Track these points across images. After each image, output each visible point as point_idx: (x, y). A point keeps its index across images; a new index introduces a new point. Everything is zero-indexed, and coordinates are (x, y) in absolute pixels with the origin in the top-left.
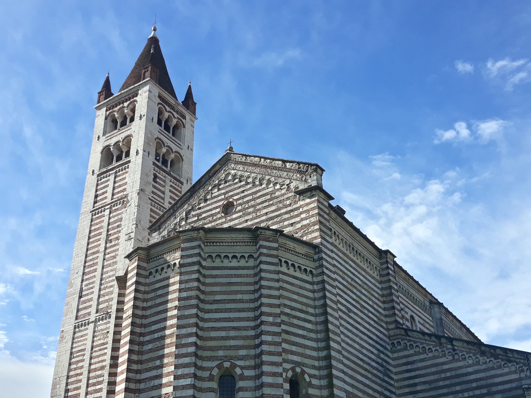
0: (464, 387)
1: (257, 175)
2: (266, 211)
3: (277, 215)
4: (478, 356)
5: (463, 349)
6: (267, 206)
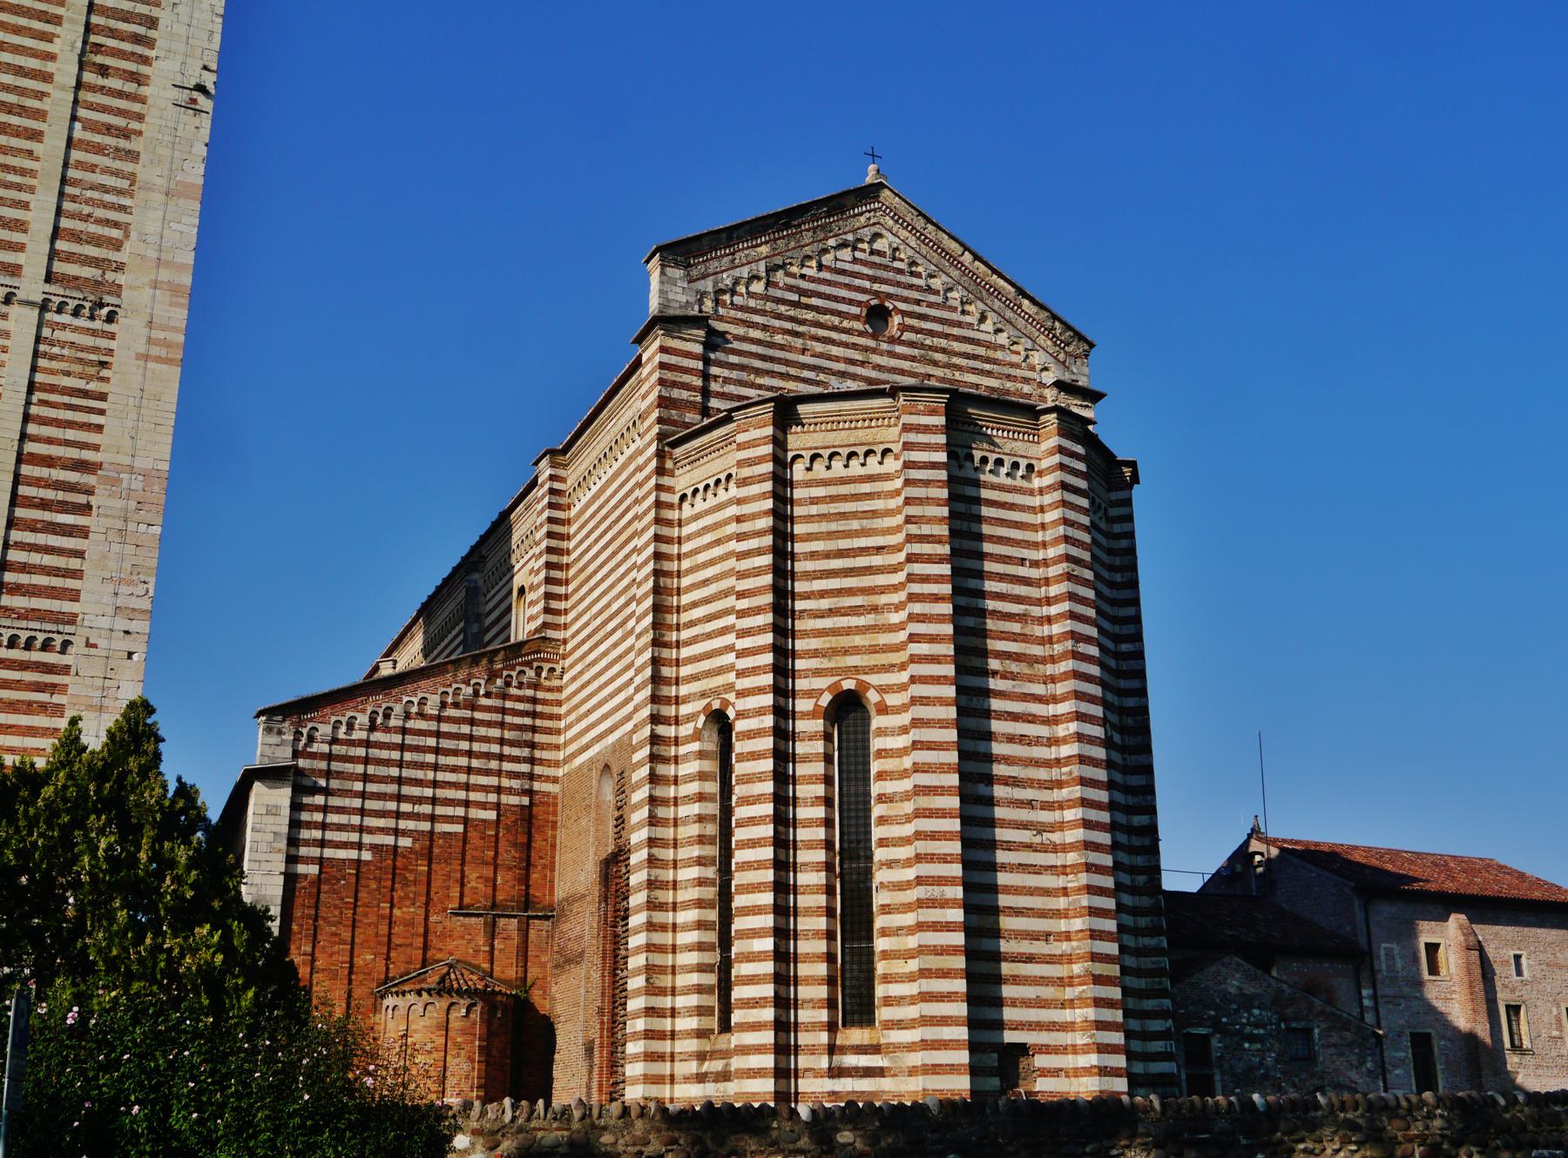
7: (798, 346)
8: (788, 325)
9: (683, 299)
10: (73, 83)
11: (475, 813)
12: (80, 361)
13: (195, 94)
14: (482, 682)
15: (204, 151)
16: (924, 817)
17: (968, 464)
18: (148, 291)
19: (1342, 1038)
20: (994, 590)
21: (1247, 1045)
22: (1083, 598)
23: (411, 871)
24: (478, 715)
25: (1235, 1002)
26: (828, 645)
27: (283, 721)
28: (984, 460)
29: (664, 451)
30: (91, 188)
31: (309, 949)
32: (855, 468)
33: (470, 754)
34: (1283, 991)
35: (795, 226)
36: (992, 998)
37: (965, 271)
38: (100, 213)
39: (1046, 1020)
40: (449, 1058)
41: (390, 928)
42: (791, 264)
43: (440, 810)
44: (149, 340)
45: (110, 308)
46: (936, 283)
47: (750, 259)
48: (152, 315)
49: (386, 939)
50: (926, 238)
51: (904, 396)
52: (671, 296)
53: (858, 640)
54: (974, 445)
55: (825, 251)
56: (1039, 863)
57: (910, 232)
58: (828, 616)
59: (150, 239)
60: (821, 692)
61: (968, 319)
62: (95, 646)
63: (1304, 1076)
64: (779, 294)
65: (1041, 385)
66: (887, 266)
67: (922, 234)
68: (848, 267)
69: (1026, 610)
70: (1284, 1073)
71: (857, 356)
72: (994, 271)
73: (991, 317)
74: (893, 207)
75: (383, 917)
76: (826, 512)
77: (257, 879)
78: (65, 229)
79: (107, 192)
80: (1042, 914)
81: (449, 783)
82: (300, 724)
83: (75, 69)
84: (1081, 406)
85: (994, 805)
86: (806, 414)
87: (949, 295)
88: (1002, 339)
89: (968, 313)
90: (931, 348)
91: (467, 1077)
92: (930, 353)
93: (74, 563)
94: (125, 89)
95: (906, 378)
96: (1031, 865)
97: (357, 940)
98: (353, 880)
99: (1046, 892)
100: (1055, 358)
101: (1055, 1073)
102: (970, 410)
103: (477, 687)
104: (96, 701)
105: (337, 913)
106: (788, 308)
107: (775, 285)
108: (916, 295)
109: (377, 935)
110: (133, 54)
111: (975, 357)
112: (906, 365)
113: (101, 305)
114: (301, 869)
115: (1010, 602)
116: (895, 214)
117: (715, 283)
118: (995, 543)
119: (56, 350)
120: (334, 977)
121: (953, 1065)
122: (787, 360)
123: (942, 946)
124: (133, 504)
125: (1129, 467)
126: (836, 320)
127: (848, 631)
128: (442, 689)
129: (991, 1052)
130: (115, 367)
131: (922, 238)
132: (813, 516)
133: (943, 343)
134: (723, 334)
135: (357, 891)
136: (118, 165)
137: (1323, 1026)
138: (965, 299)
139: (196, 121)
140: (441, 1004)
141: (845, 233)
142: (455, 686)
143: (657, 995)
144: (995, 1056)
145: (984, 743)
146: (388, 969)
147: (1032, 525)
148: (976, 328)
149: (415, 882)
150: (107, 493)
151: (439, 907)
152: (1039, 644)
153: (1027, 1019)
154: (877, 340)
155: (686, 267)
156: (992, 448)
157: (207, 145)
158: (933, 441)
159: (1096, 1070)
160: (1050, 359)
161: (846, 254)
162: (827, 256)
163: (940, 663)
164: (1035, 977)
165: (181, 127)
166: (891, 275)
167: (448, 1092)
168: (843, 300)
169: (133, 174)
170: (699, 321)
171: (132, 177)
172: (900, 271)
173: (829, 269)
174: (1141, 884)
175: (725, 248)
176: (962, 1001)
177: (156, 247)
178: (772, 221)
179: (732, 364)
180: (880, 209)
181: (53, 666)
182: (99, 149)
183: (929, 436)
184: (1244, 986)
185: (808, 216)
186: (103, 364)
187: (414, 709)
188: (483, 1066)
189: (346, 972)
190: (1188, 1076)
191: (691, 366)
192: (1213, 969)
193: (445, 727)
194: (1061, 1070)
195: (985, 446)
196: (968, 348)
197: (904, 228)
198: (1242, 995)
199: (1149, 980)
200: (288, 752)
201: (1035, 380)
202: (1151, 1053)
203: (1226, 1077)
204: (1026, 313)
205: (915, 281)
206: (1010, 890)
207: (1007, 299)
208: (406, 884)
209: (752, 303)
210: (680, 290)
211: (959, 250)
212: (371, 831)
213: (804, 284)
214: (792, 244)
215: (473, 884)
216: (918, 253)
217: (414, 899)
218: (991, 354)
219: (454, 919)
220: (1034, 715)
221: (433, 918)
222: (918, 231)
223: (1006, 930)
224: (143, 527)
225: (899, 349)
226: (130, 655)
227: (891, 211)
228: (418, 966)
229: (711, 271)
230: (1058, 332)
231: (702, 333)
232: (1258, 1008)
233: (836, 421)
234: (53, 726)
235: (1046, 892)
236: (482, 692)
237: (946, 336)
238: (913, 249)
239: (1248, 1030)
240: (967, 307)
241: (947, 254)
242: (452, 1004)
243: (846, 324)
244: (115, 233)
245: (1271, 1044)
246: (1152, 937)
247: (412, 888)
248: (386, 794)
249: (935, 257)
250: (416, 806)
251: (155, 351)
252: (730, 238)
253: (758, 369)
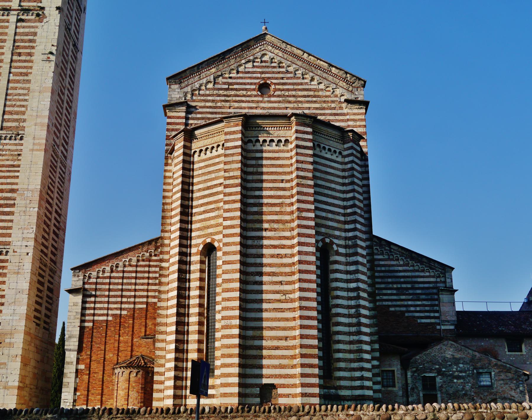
0: (394, 280)
4: (409, 260)
5: (398, 253)
7: (227, 106)
8: (223, 98)
9: (178, 96)
10: (10, 61)
11: (151, 300)
12: (12, 155)
13: (49, 55)
14: (153, 251)
15: (52, 74)
16: (225, 292)
17: (258, 144)
18: (33, 127)
19: (506, 376)
20: (267, 194)
21: (455, 381)
23: (126, 323)
24: (152, 263)
25: (450, 361)
26: (202, 226)
27: (79, 272)
28: (265, 141)
29: (168, 157)
30: (15, 95)
31: (89, 353)
32: (214, 153)
33: (148, 278)
34: (476, 356)
35: (227, 58)
36: (258, 365)
38: (18, 103)
39: (284, 374)
40: (130, 392)
41: (119, 344)
42: (225, 74)
43: (119, 299)
44: (34, 144)
45: (21, 135)
46: (291, 69)
47: (207, 75)
48: (34, 135)
49: (117, 348)
50: (287, 51)
52: (173, 96)
53: (212, 222)
54: (259, 136)
55: (241, 65)
56: (283, 307)
57: (280, 50)
58: (203, 214)
59: (34, 109)
60: (199, 244)
61: (306, 81)
62: (16, 252)
63: (486, 394)
64: (219, 86)
65: (340, 102)
66: (268, 66)
67: (285, 50)
68: (250, 70)
69: (283, 201)
70: (475, 393)
71: (254, 105)
72: (318, 59)
73: (317, 78)
74: (272, 42)
75: (115, 340)
77: (70, 329)
78: (7, 111)
79: (20, 96)
80: (284, 329)
81: (141, 289)
82: (85, 272)
83: (10, 56)
84: (359, 108)
85: (262, 284)
87: (297, 73)
88: (322, 86)
89: (306, 78)
90: (288, 96)
91: (136, 399)
92: (287, 98)
93: (10, 224)
94: (27, 59)
96: (280, 309)
97: (106, 349)
98: (105, 327)
99: (287, 320)
101: (287, 396)
102: (258, 121)
103: (151, 253)
104: (16, 271)
105: (99, 339)
106: (224, 91)
107: (218, 83)
109: (114, 347)
110: (29, 46)
111: (308, 96)
112: (276, 105)
113: (18, 135)
114: (86, 324)
116: (273, 44)
117: (192, 88)
118: (269, 175)
119: (4, 153)
120: (98, 363)
121: (232, 393)
122: (222, 112)
123: (230, 344)
124: (28, 202)
126: (244, 92)
127: (209, 219)
128: (137, 255)
129: (256, 387)
130: (23, 155)
131: (285, 51)
133: (294, 93)
134: (195, 107)
135: (106, 332)
136: (24, 85)
137: (497, 371)
138: (304, 73)
139: (50, 65)
140: (127, 371)
141: (249, 57)
142: (142, 253)
143: (159, 367)
144: (258, 389)
145: (260, 259)
146: (118, 359)
147: (287, 165)
149: (128, 327)
150: (20, 199)
151: (137, 336)
152: (288, 215)
153: (274, 373)
154: (263, 97)
156: (268, 135)
157: (53, 72)
158: (236, 137)
159: (300, 395)
161: (250, 65)
162: (242, 67)
163: (234, 228)
164: (279, 356)
165: (44, 68)
166: (270, 70)
167: (129, 404)
169: (29, 88)
170: (184, 103)
171: (28, 89)
172: (274, 67)
173: (242, 72)
174: (353, 313)
175: (196, 73)
176: (237, 367)
177: (36, 111)
178: (217, 58)
179: (198, 118)
180: (266, 43)
181: (3, 260)
182: (18, 82)
183: (234, 135)
184: (455, 354)
185: (232, 53)
186: (19, 155)
187: (127, 263)
188: (143, 395)
189: (102, 361)
190: (423, 395)
191: (180, 122)
192: (438, 347)
193: (139, 269)
194: (290, 394)
195: (265, 135)
196: (306, 93)
197: (276, 49)
198: (454, 358)
199: (356, 354)
200: (81, 283)
202: (356, 386)
203: (444, 395)
204: (333, 73)
205: (281, 70)
206: (268, 320)
207: (324, 69)
208: (125, 327)
209: (208, 92)
210: (177, 93)
211: (302, 53)
212: (112, 309)
214: (226, 65)
215: (150, 326)
216: (283, 58)
217: (128, 333)
218: (316, 93)
219: (142, 340)
220: (284, 245)
221: (135, 340)
223: (266, 337)
224: (32, 209)
225: (273, 99)
226: (28, 254)
227: (271, 43)
228: (129, 358)
229: (189, 83)
230: (349, 78)
231: (184, 108)
232: (462, 363)
233: (208, 136)
234: (3, 280)
235: (287, 320)
236: (153, 254)
237: (295, 90)
238: (280, 57)
239: (456, 374)
240: (305, 76)
241: (294, 55)
242: (131, 372)
243: (249, 93)
244: (23, 109)
245: (468, 380)
246: (357, 336)
247: (127, 329)
248: (117, 295)
249: (291, 58)
250: (129, 299)
251: (36, 147)
252: (198, 69)
253: (209, 118)
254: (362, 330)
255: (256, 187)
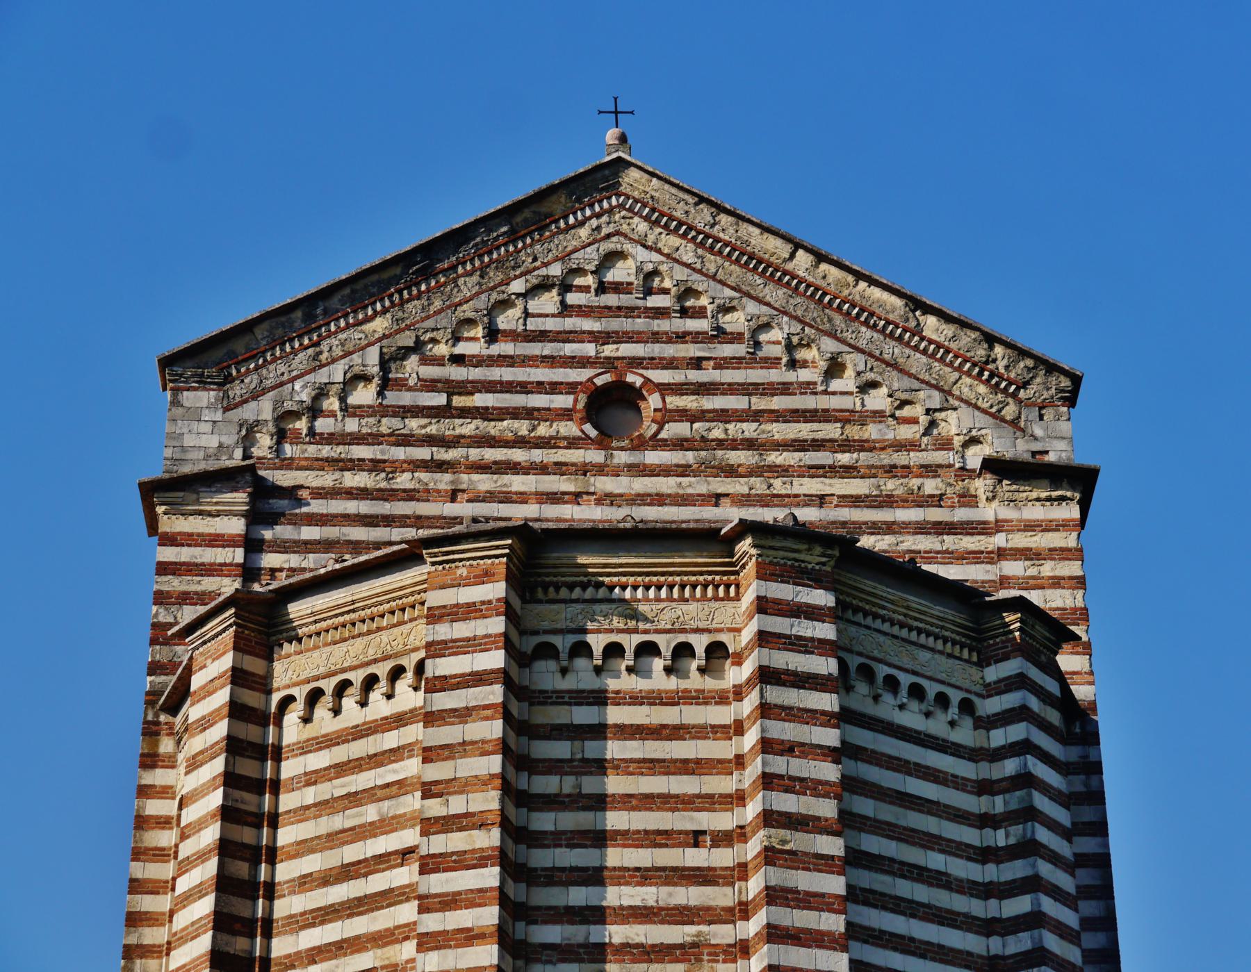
1: (773, 317)
2: (820, 486)
3: (874, 523)
6: (823, 467)
7: (442, 486)
8: (423, 453)
9: (213, 442)
17: (581, 663)
20: (626, 902)
22: (807, 893)
28: (614, 650)
29: (157, 723)
32: (379, 706)
35: (444, 271)
37: (794, 284)
42: (434, 341)
47: (350, 346)
50: (717, 240)
51: (430, 554)
52: (189, 441)
54: (590, 626)
55: (505, 304)
57: (684, 236)
61: (804, 375)
64: (406, 398)
65: (964, 473)
66: (632, 309)
67: (707, 236)
68: (551, 325)
69: (699, 934)
72: (859, 276)
73: (853, 362)
74: (647, 198)
76: (328, 796)
84: (1049, 499)
86: (302, 618)
87: (763, 337)
88: (878, 400)
89: (805, 364)
90: (721, 444)
92: (720, 453)
95: (666, 509)
100: (997, 416)
102: (582, 560)
106: (424, 421)
107: (401, 385)
108: (693, 350)
111: (817, 445)
112: (666, 485)
115: (662, 922)
116: (653, 210)
117: (278, 403)
118: (633, 809)
122: (419, 517)
125: (1015, 611)
126: (522, 427)
131: (706, 242)
132: (308, 807)
133: (749, 429)
134: (291, 493)
138: (795, 340)
141: (546, 265)
147: (720, 761)
148: (820, 388)
154: (606, 448)
155: (221, 385)
156: (631, 624)
160: (982, 419)
161: (548, 302)
162: (510, 312)
166: (640, 324)
168: (540, 388)
172: (660, 313)
173: (513, 336)
175: (300, 337)
178: (398, 270)
179: (306, 543)
180: (621, 206)
185: (469, 249)
191: (220, 560)
195: (617, 622)
196: (803, 430)
197: (670, 232)
201: (950, 466)
204: (931, 342)
207: (888, 322)
209: (352, 425)
210: (207, 427)
211: (784, 249)
213: (457, 373)
214: (438, 304)
216: (700, 272)
218: (853, 432)
222: (699, 232)
225: (653, 457)
227: (645, 205)
229: (268, 383)
230: (1001, 365)
231: (239, 498)
237: (755, 416)
238: (688, 266)
240: (802, 354)
241: (751, 257)
243: (543, 430)
249: (734, 273)
252: (309, 317)
253: (358, 543)
254: (833, 627)
255: (573, 869)
